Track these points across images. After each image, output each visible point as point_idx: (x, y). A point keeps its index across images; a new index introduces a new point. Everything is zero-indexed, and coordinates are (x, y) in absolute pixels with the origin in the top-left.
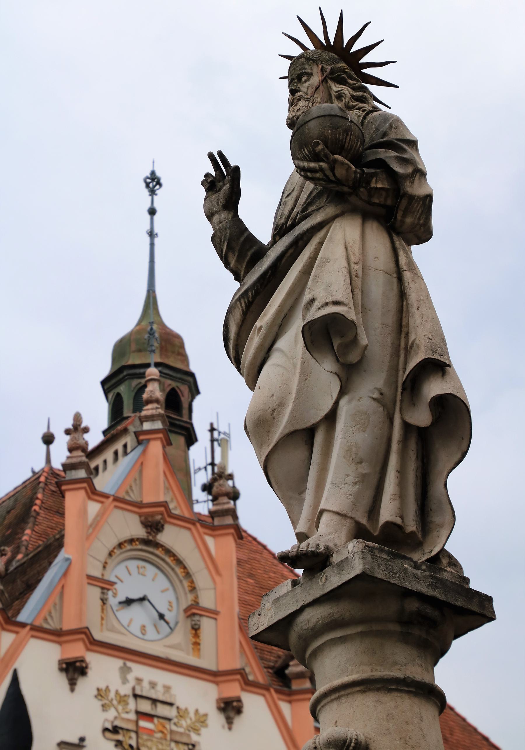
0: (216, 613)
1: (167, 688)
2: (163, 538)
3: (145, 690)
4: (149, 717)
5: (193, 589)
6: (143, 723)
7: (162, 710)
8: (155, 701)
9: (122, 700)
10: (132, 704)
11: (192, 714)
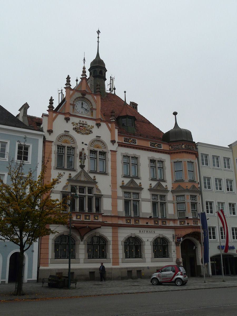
0: (96, 109)
1: (86, 122)
2: (86, 97)
3: (82, 122)
4: (82, 127)
5: (92, 105)
6: (81, 128)
7: (84, 125)
8: (83, 124)
9: (77, 124)
10: (79, 125)
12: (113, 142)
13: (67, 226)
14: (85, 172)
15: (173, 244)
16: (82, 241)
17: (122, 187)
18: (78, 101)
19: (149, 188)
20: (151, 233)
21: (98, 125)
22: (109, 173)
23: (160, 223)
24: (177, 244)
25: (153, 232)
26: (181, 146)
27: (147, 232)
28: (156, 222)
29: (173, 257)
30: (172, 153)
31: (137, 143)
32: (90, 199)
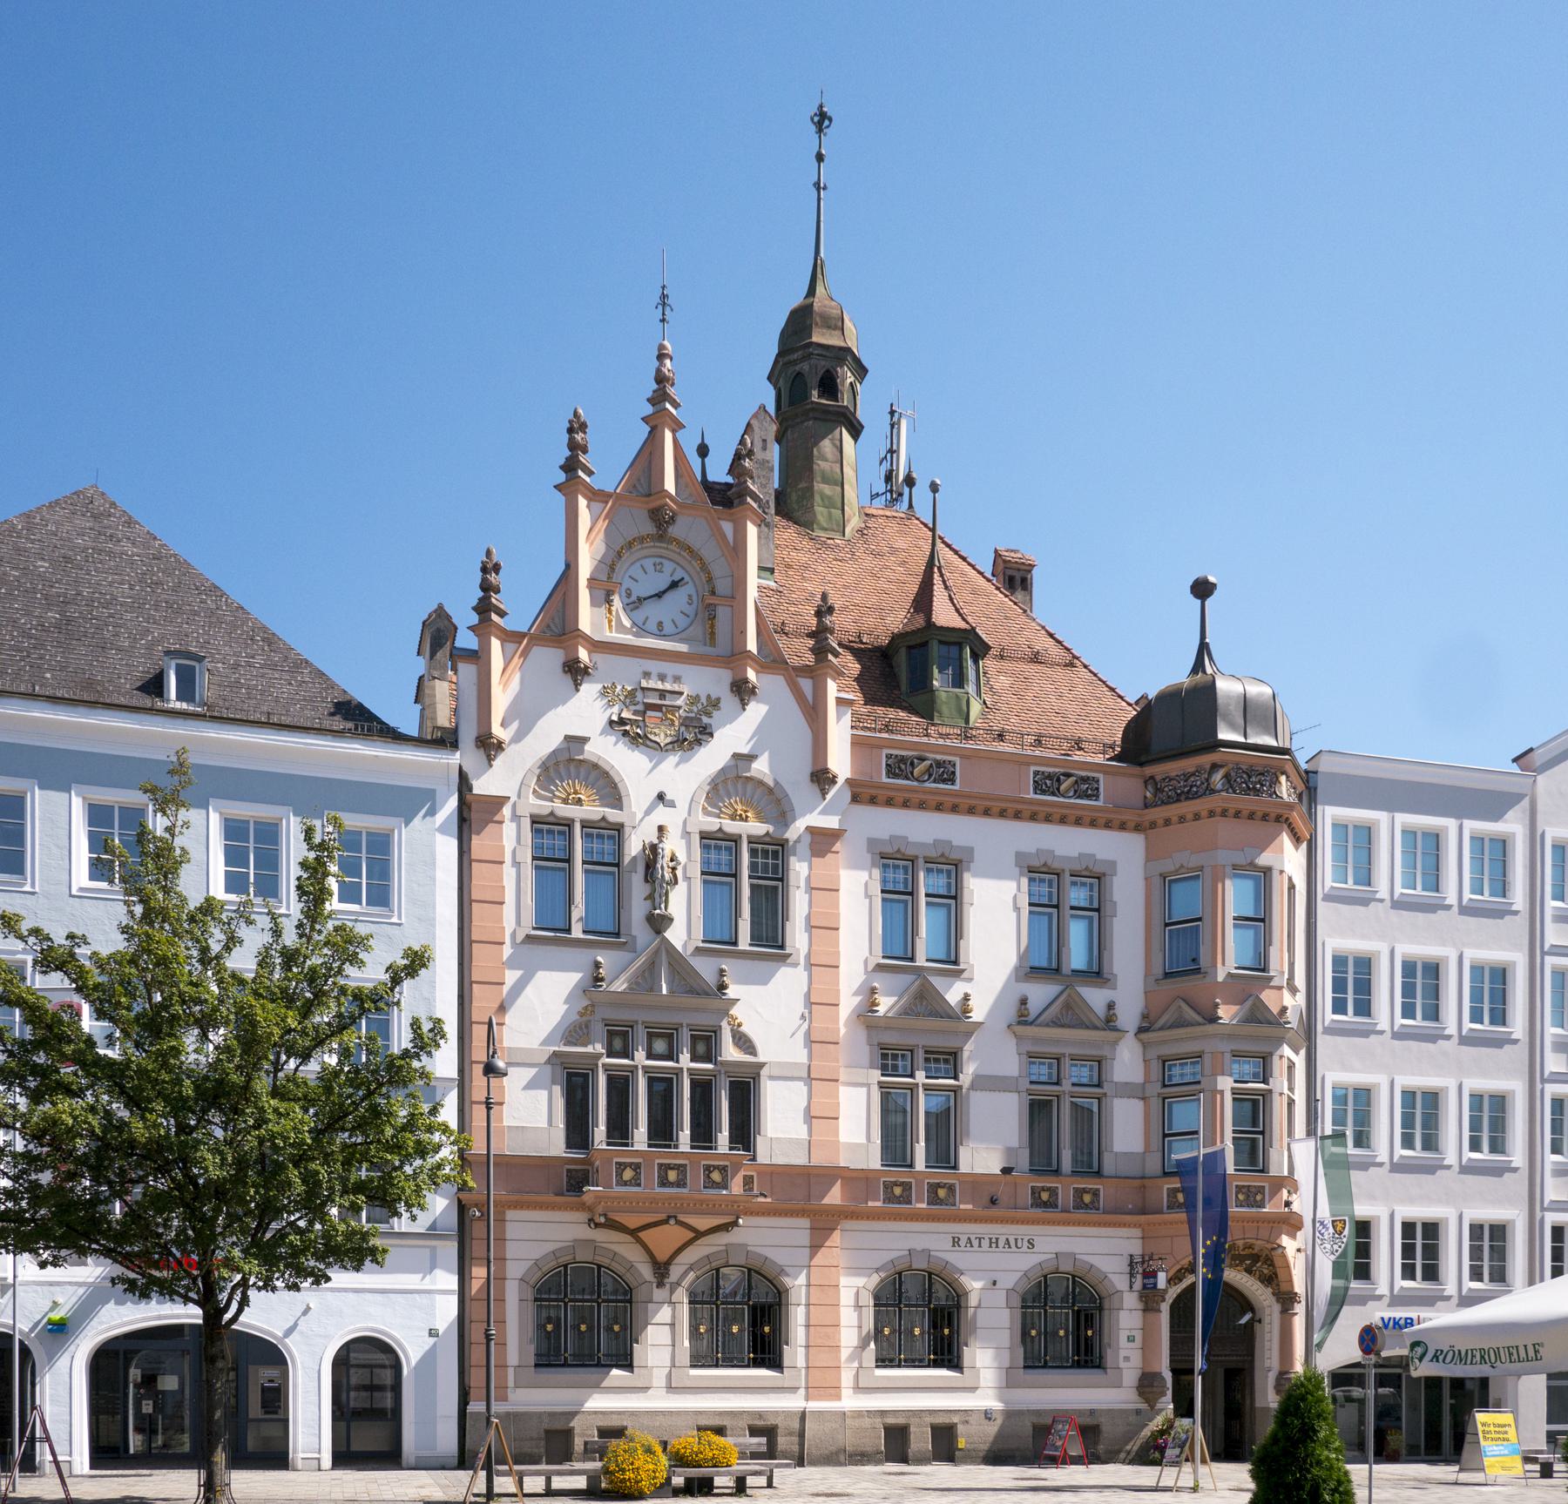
11: (704, 700)
13: (589, 1220)
15: (1131, 1300)
16: (660, 1285)
18: (638, 564)
22: (798, 950)
24: (1150, 1298)
25: (1026, 1244)
26: (1207, 780)
27: (994, 1243)
29: (1122, 1364)
30: (1153, 825)
31: (958, 781)
32: (703, 1091)
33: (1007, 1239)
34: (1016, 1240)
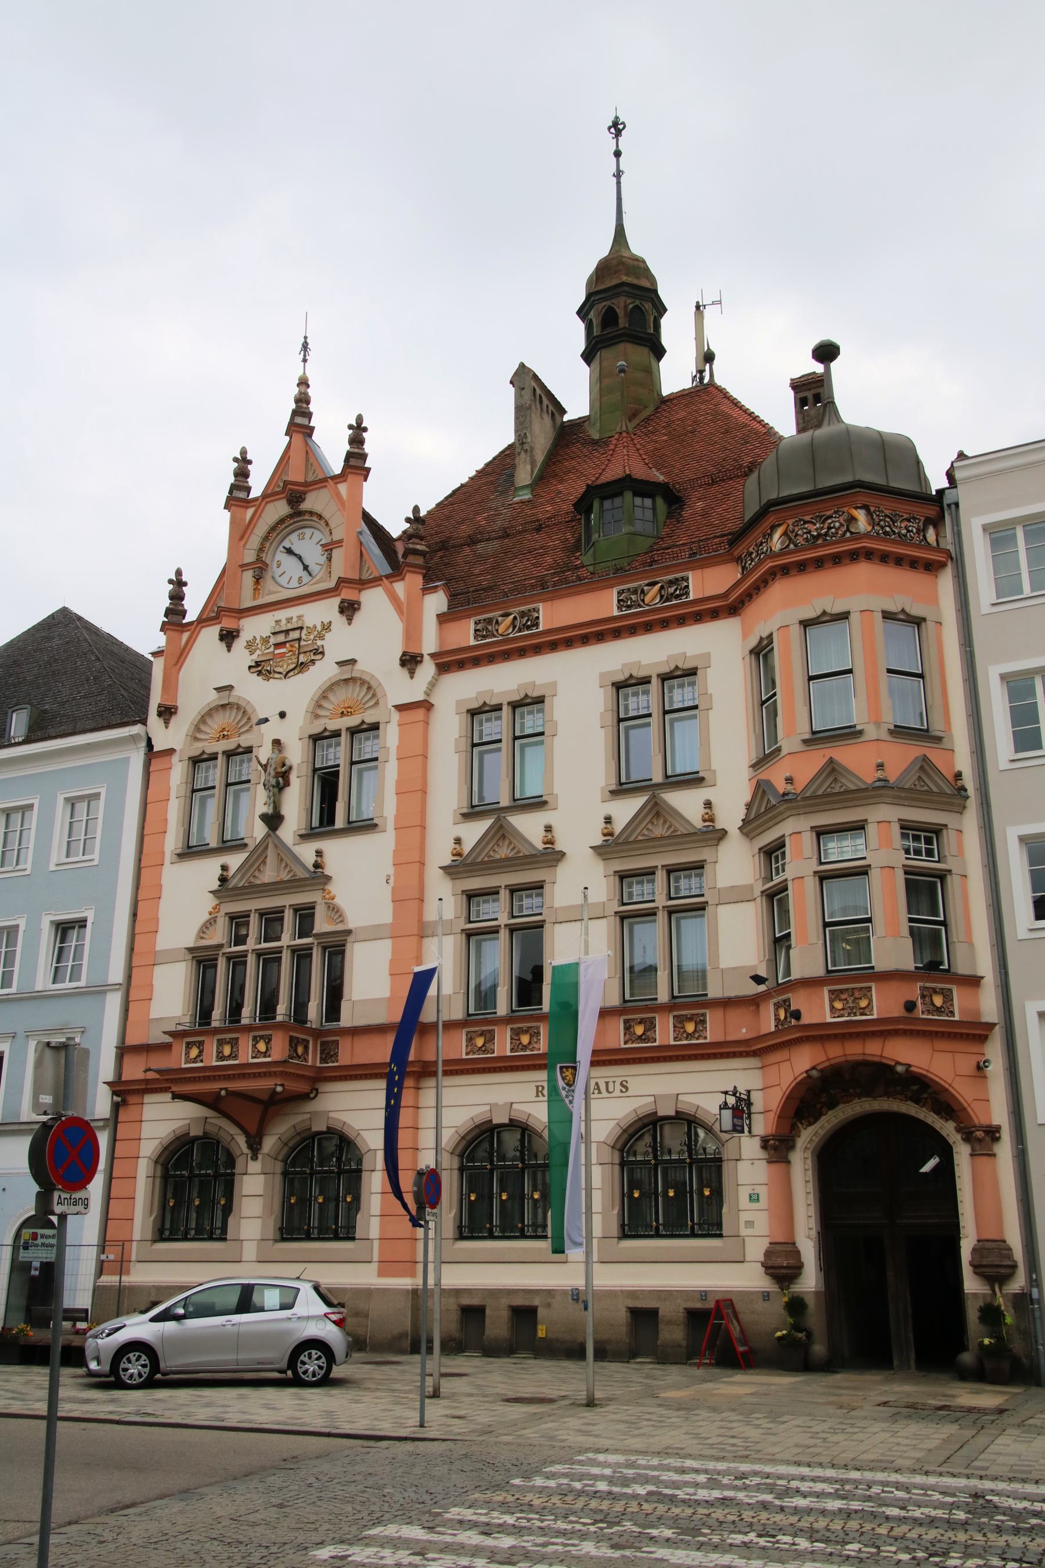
12: (410, 661)
14: (280, 845)
17: (451, 871)
19: (598, 840)
20: (605, 1094)
21: (349, 609)
23: (665, 1033)
25: (618, 1087)
28: (639, 1030)
33: (597, 1084)
34: (607, 1083)
